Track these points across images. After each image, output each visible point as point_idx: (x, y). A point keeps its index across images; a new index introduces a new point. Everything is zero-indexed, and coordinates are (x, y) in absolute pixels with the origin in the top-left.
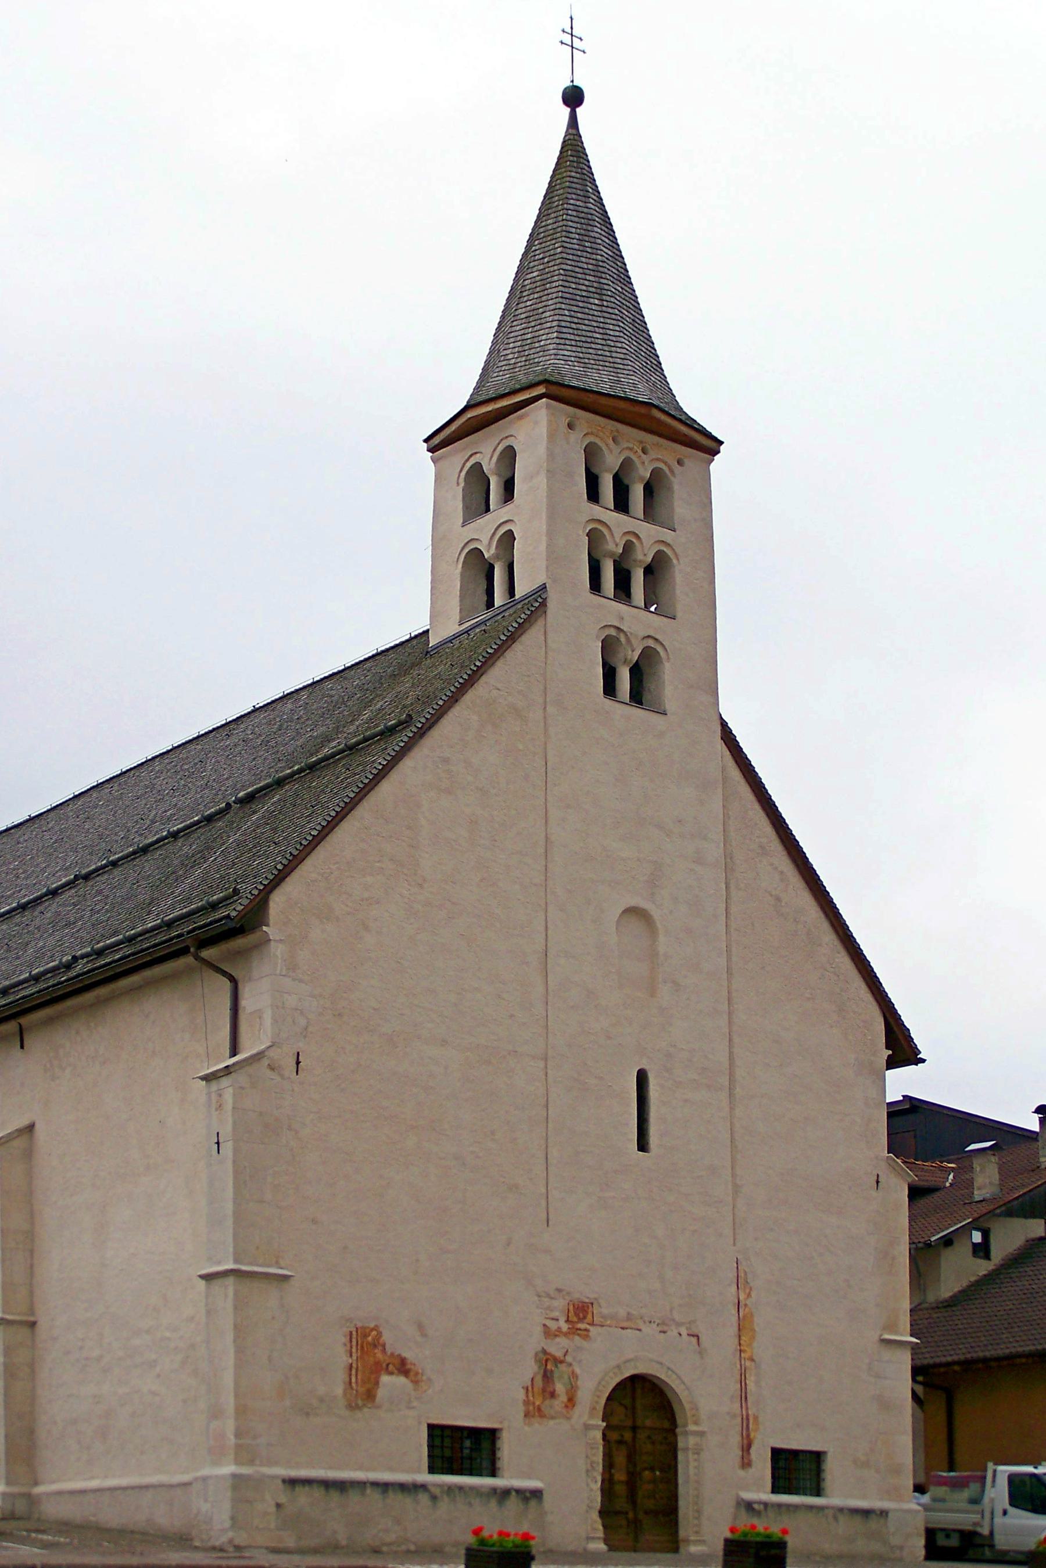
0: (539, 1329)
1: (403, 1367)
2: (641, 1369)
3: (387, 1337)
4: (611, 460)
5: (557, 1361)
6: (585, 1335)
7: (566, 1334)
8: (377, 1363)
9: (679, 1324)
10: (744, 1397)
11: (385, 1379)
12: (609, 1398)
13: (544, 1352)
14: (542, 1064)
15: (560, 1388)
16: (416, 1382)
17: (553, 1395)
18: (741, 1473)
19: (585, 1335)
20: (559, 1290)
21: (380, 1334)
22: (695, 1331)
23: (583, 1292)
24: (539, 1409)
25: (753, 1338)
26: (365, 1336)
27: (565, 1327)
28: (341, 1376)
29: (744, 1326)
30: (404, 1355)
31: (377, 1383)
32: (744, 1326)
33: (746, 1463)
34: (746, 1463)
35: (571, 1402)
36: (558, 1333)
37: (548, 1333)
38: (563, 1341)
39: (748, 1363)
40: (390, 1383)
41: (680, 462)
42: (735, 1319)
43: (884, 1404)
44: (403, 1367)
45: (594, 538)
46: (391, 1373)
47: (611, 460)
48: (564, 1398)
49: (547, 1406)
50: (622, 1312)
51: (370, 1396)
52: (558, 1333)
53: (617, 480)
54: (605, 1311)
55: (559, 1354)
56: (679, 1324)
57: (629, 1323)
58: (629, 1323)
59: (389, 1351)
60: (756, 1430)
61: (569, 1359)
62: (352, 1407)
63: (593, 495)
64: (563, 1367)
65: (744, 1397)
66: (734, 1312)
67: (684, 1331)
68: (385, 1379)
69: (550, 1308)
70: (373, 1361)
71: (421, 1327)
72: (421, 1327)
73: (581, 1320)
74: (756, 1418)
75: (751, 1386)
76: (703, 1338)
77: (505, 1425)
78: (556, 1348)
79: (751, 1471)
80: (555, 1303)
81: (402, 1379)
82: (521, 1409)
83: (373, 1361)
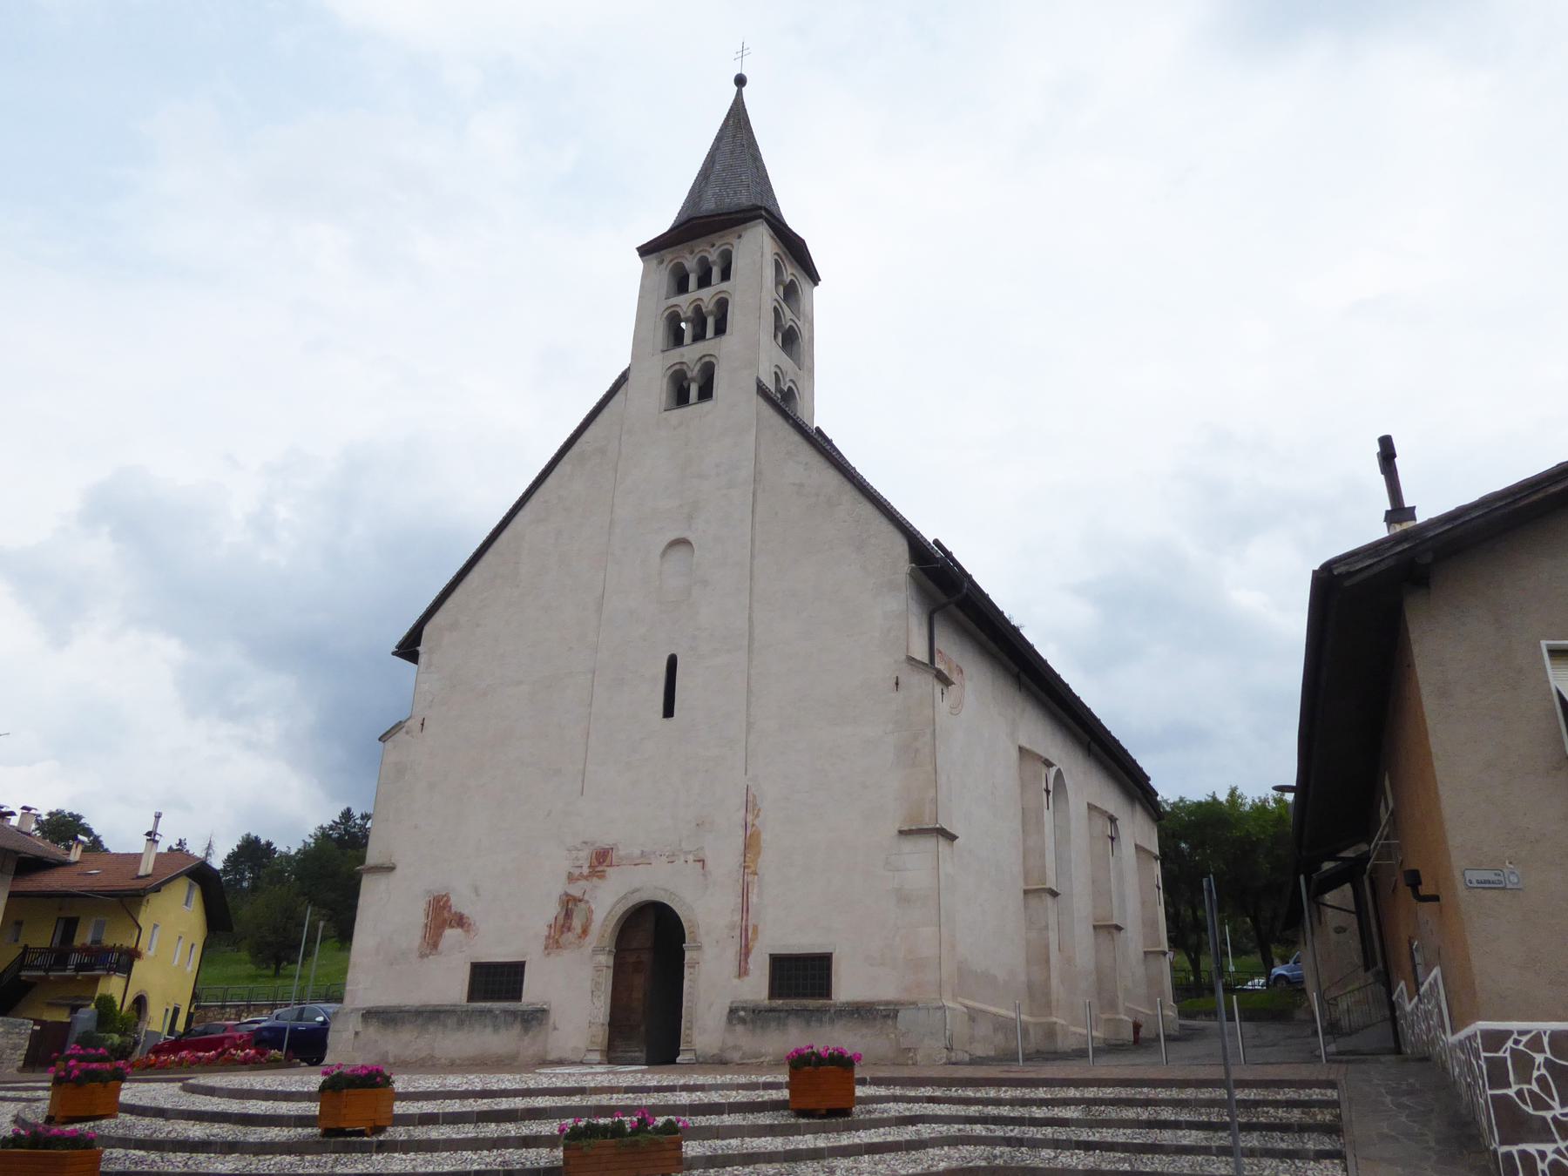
2: (646, 896)
3: (453, 900)
4: (691, 263)
5: (577, 900)
7: (586, 878)
8: (445, 921)
10: (745, 908)
13: (567, 894)
15: (577, 923)
17: (569, 929)
18: (736, 981)
22: (701, 856)
23: (604, 841)
27: (586, 871)
29: (751, 844)
30: (466, 912)
32: (751, 844)
33: (743, 972)
34: (743, 972)
35: (585, 932)
37: (571, 878)
38: (582, 883)
39: (750, 878)
40: (451, 934)
44: (460, 921)
47: (691, 263)
48: (579, 930)
50: (637, 852)
51: (435, 946)
54: (622, 853)
56: (686, 853)
57: (644, 859)
60: (754, 939)
62: (422, 956)
64: (582, 905)
65: (745, 908)
66: (742, 833)
67: (691, 858)
68: (448, 932)
69: (577, 859)
71: (476, 890)
72: (476, 890)
74: (755, 928)
75: (753, 899)
76: (709, 863)
78: (575, 891)
79: (746, 979)
82: (542, 941)
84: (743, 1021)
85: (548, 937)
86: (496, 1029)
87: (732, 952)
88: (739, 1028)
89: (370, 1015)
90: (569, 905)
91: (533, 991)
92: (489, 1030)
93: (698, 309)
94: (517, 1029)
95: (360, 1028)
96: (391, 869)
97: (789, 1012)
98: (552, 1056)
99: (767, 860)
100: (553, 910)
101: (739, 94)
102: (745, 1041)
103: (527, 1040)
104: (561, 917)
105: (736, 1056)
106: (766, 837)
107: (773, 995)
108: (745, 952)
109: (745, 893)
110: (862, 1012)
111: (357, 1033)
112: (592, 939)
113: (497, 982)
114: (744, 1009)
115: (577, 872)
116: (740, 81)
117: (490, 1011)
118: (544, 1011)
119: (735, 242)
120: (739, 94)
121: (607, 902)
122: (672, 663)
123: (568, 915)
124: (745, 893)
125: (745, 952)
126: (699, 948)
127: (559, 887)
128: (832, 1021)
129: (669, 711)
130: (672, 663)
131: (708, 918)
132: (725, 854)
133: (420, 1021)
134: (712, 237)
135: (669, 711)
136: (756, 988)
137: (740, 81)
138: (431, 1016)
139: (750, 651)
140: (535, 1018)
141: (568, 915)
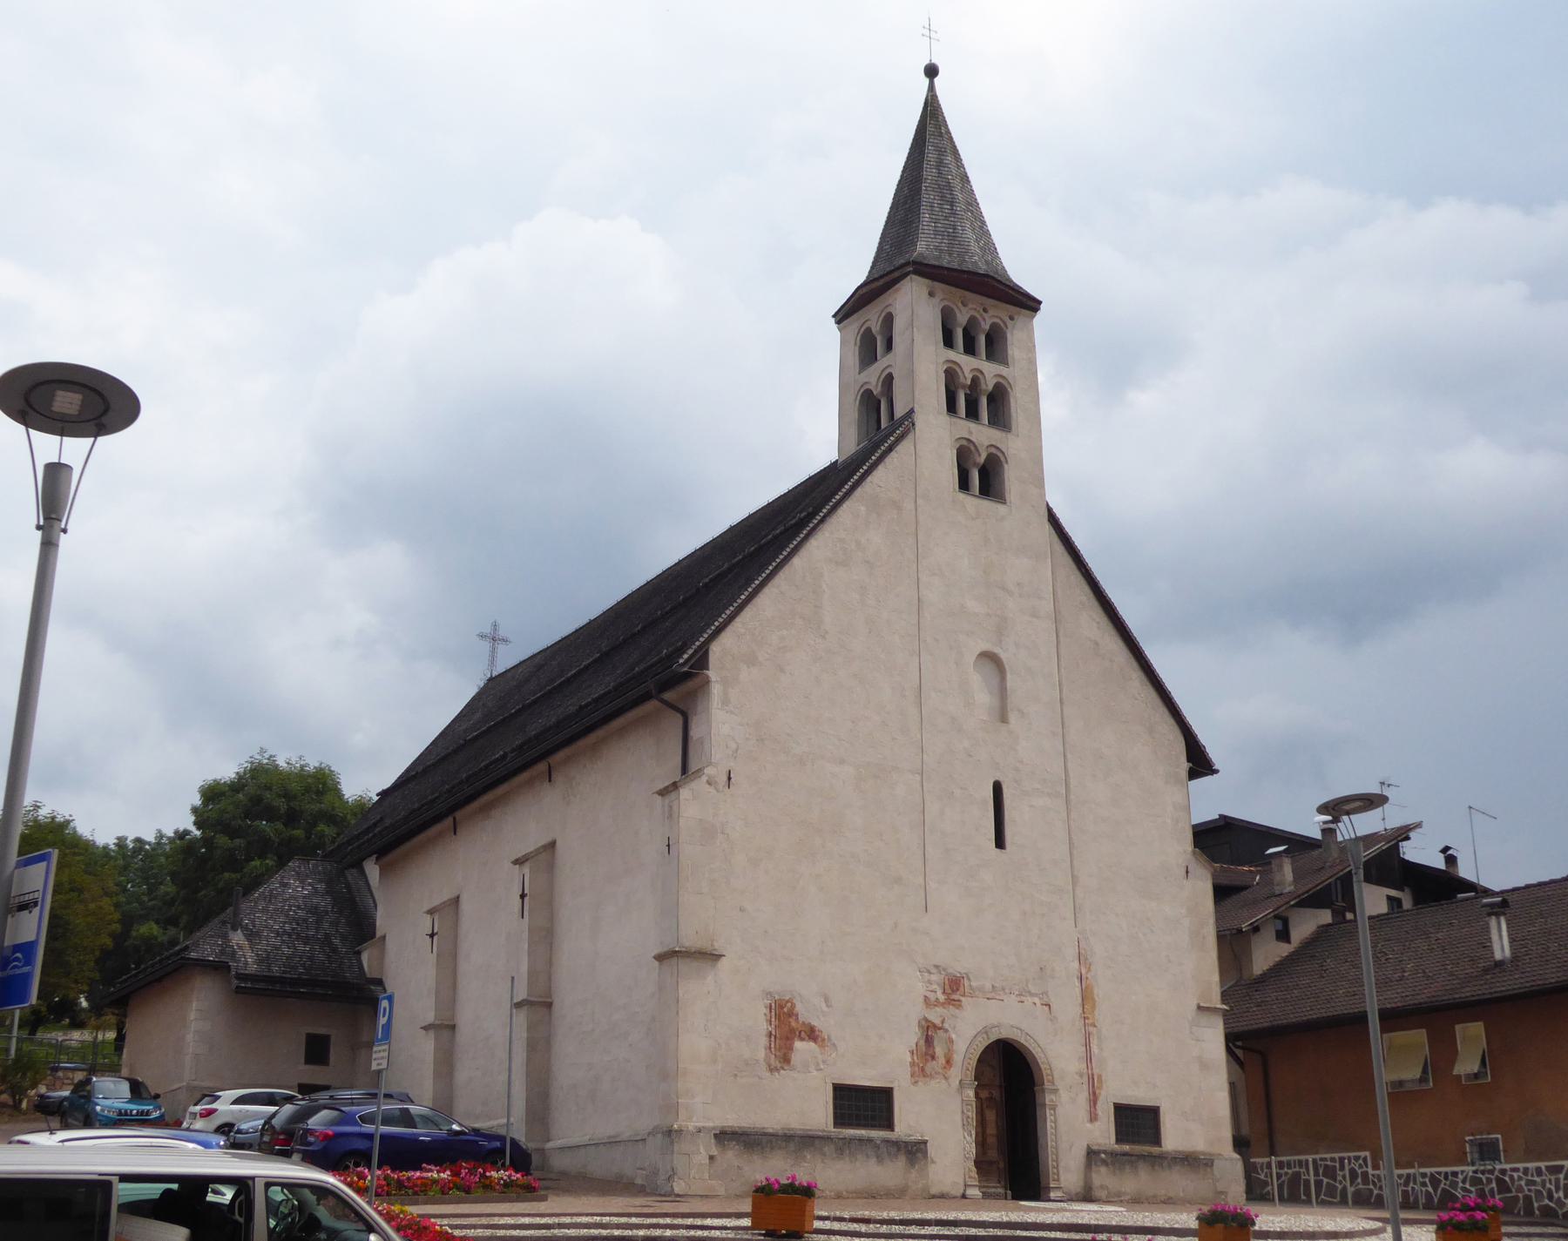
0: (921, 1000)
1: (812, 1034)
2: (1005, 1034)
3: (799, 1008)
4: (962, 317)
6: (957, 1004)
8: (792, 1031)
9: (1032, 995)
11: (798, 1044)
12: (981, 1060)
13: (926, 1020)
14: (918, 778)
15: (939, 1050)
16: (822, 1046)
17: (933, 1058)
19: (957, 1004)
20: (937, 967)
21: (793, 1006)
23: (957, 968)
24: (923, 1070)
25: (1093, 1007)
26: (782, 1007)
27: (942, 998)
28: (764, 1041)
29: (1087, 997)
30: (815, 1023)
31: (791, 1048)
32: (1087, 997)
33: (1093, 1118)
36: (937, 1003)
38: (939, 1010)
41: (1012, 318)
42: (1078, 990)
43: (1204, 1065)
44: (812, 1034)
45: (951, 376)
46: (802, 1039)
47: (962, 317)
48: (942, 1060)
49: (931, 1066)
50: (988, 986)
51: (786, 1060)
52: (937, 1003)
53: (966, 331)
55: (938, 1022)
58: (994, 993)
59: (801, 1019)
60: (1100, 1088)
61: (946, 1026)
63: (948, 342)
64: (940, 1033)
66: (1077, 984)
68: (798, 1044)
69: (930, 982)
70: (788, 1029)
71: (827, 1000)
73: (954, 991)
74: (1100, 1077)
75: (1095, 1049)
76: (1054, 1007)
77: (894, 1085)
78: (934, 1016)
79: (1097, 1124)
80: (934, 978)
81: (812, 1044)
83: (788, 1029)
84: (1104, 1162)
85: (913, 1064)
86: (880, 1160)
87: (1083, 1097)
88: (1103, 1169)
89: (725, 1136)
90: (929, 1032)
91: (909, 1118)
92: (873, 1160)
93: (975, 380)
94: (901, 1161)
95: (714, 1152)
96: (712, 957)
97: (1142, 1157)
98: (934, 1191)
99: (1102, 1014)
100: (913, 1036)
101: (931, 87)
102: (1103, 1178)
103: (914, 1174)
104: (922, 1042)
105: (1103, 1194)
106: (1099, 992)
107: (1118, 1141)
108: (1094, 1099)
109: (1087, 1045)
110: (1190, 1161)
111: (711, 1158)
112: (956, 1074)
113: (863, 1107)
114: (1105, 1152)
115: (932, 996)
116: (931, 71)
117: (870, 1140)
118: (925, 1142)
119: (1009, 323)
120: (931, 87)
121: (968, 1032)
122: (998, 789)
123: (929, 1041)
124: (1087, 1045)
125: (1094, 1099)
126: (1056, 1091)
127: (917, 1011)
128: (1170, 1166)
129: (1000, 843)
130: (998, 789)
131: (1058, 1057)
132: (1067, 1004)
133: (792, 1146)
134: (989, 302)
135: (1000, 843)
136: (1104, 1133)
137: (931, 71)
138: (802, 1142)
139: (1068, 801)
140: (915, 1151)
141: (929, 1041)
